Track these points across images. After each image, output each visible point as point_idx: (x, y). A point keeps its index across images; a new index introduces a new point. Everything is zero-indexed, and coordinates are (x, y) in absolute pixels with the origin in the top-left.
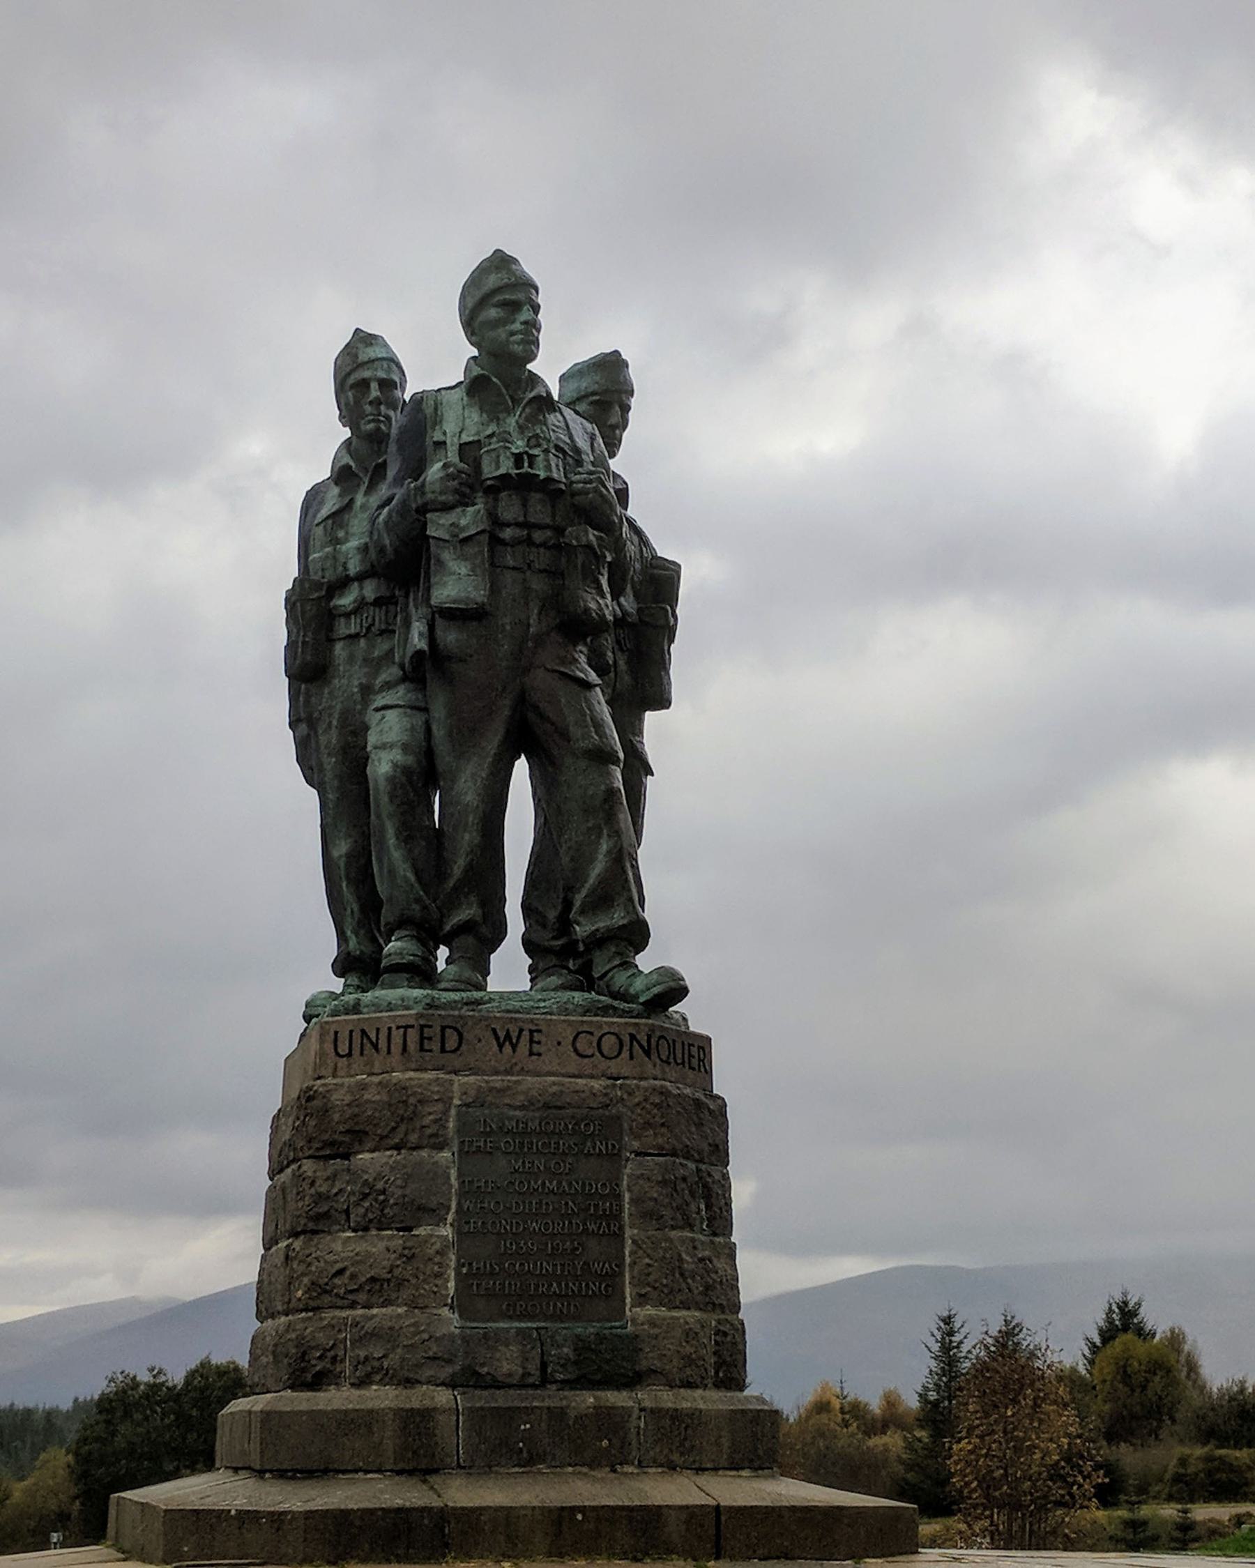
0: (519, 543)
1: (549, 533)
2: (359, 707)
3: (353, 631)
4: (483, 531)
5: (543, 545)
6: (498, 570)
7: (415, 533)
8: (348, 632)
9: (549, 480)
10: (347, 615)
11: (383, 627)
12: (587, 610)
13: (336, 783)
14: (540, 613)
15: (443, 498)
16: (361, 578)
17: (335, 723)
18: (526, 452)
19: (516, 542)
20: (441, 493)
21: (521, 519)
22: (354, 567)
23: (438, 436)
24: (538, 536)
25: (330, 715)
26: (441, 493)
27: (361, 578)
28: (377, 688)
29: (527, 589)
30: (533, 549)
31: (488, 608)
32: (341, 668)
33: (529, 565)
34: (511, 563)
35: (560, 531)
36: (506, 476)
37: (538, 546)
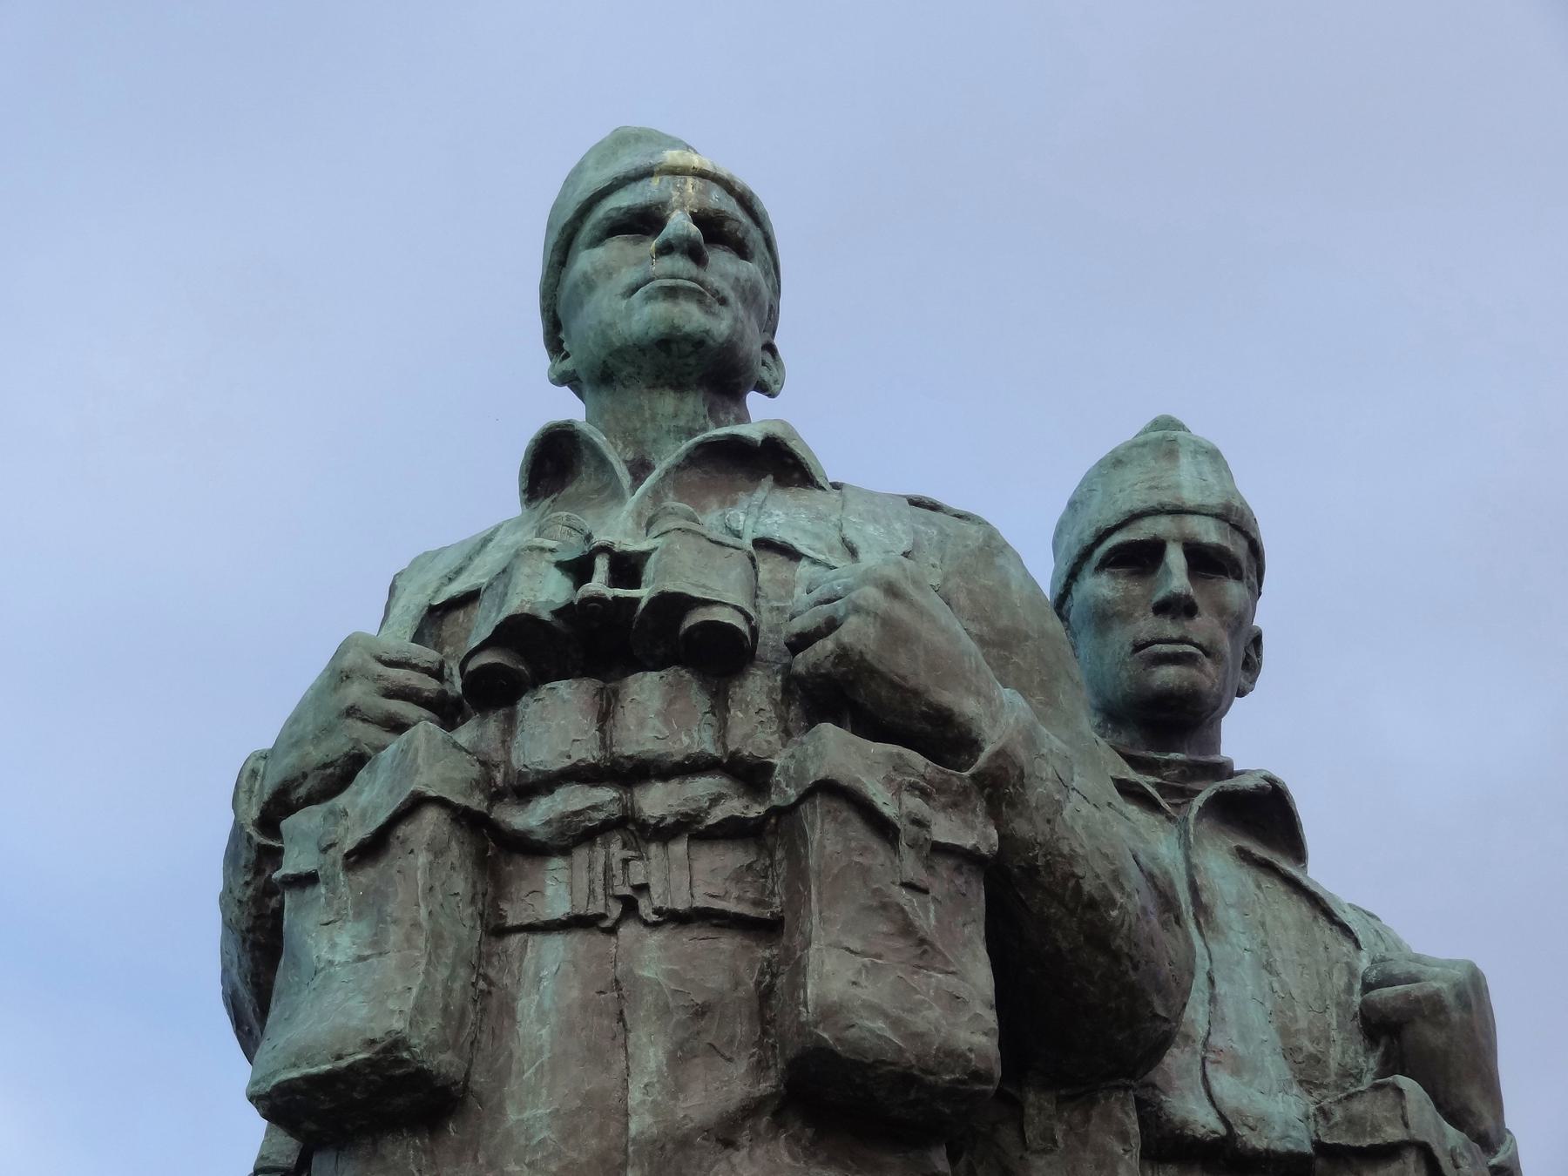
0: (589, 836)
1: (702, 787)
4: (416, 804)
5: (687, 828)
6: (514, 940)
9: (674, 605)
12: (829, 1012)
14: (680, 1057)
18: (605, 549)
19: (574, 836)
20: (317, 740)
21: (587, 752)
24: (656, 801)
26: (317, 740)
29: (616, 1000)
30: (654, 849)
31: (445, 1062)
33: (629, 907)
34: (557, 904)
35: (750, 775)
36: (517, 632)
37: (663, 833)
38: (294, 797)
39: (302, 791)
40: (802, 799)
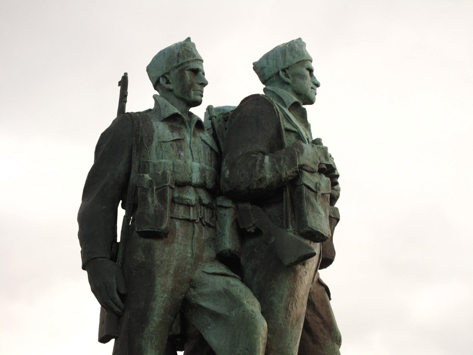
2: (189, 267)
3: (192, 217)
7: (290, 178)
8: (187, 217)
10: (188, 206)
11: (208, 222)
13: (162, 311)
15: (313, 166)
16: (196, 187)
17: (171, 272)
22: (196, 178)
23: (289, 126)
25: (168, 266)
27: (196, 187)
28: (204, 259)
32: (180, 238)
38: (304, 167)
39: (306, 168)
40: (334, 218)
